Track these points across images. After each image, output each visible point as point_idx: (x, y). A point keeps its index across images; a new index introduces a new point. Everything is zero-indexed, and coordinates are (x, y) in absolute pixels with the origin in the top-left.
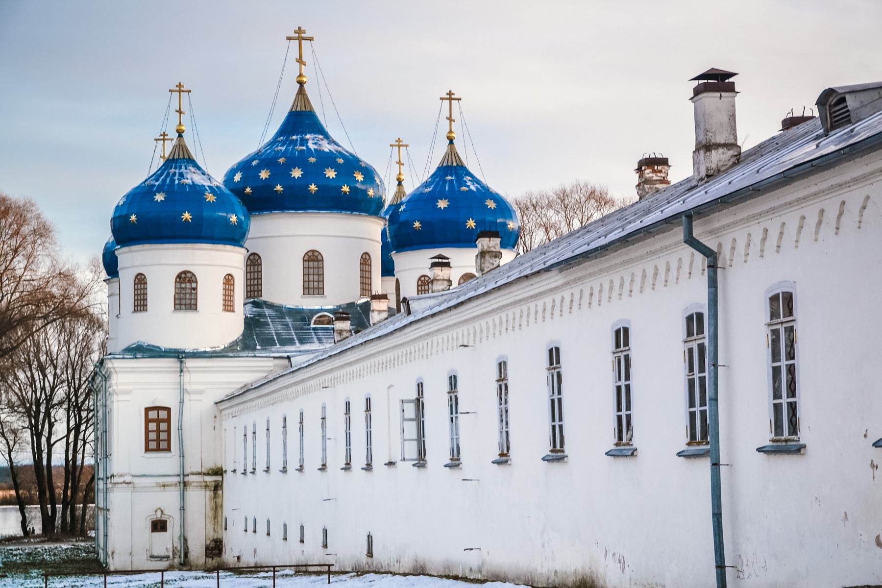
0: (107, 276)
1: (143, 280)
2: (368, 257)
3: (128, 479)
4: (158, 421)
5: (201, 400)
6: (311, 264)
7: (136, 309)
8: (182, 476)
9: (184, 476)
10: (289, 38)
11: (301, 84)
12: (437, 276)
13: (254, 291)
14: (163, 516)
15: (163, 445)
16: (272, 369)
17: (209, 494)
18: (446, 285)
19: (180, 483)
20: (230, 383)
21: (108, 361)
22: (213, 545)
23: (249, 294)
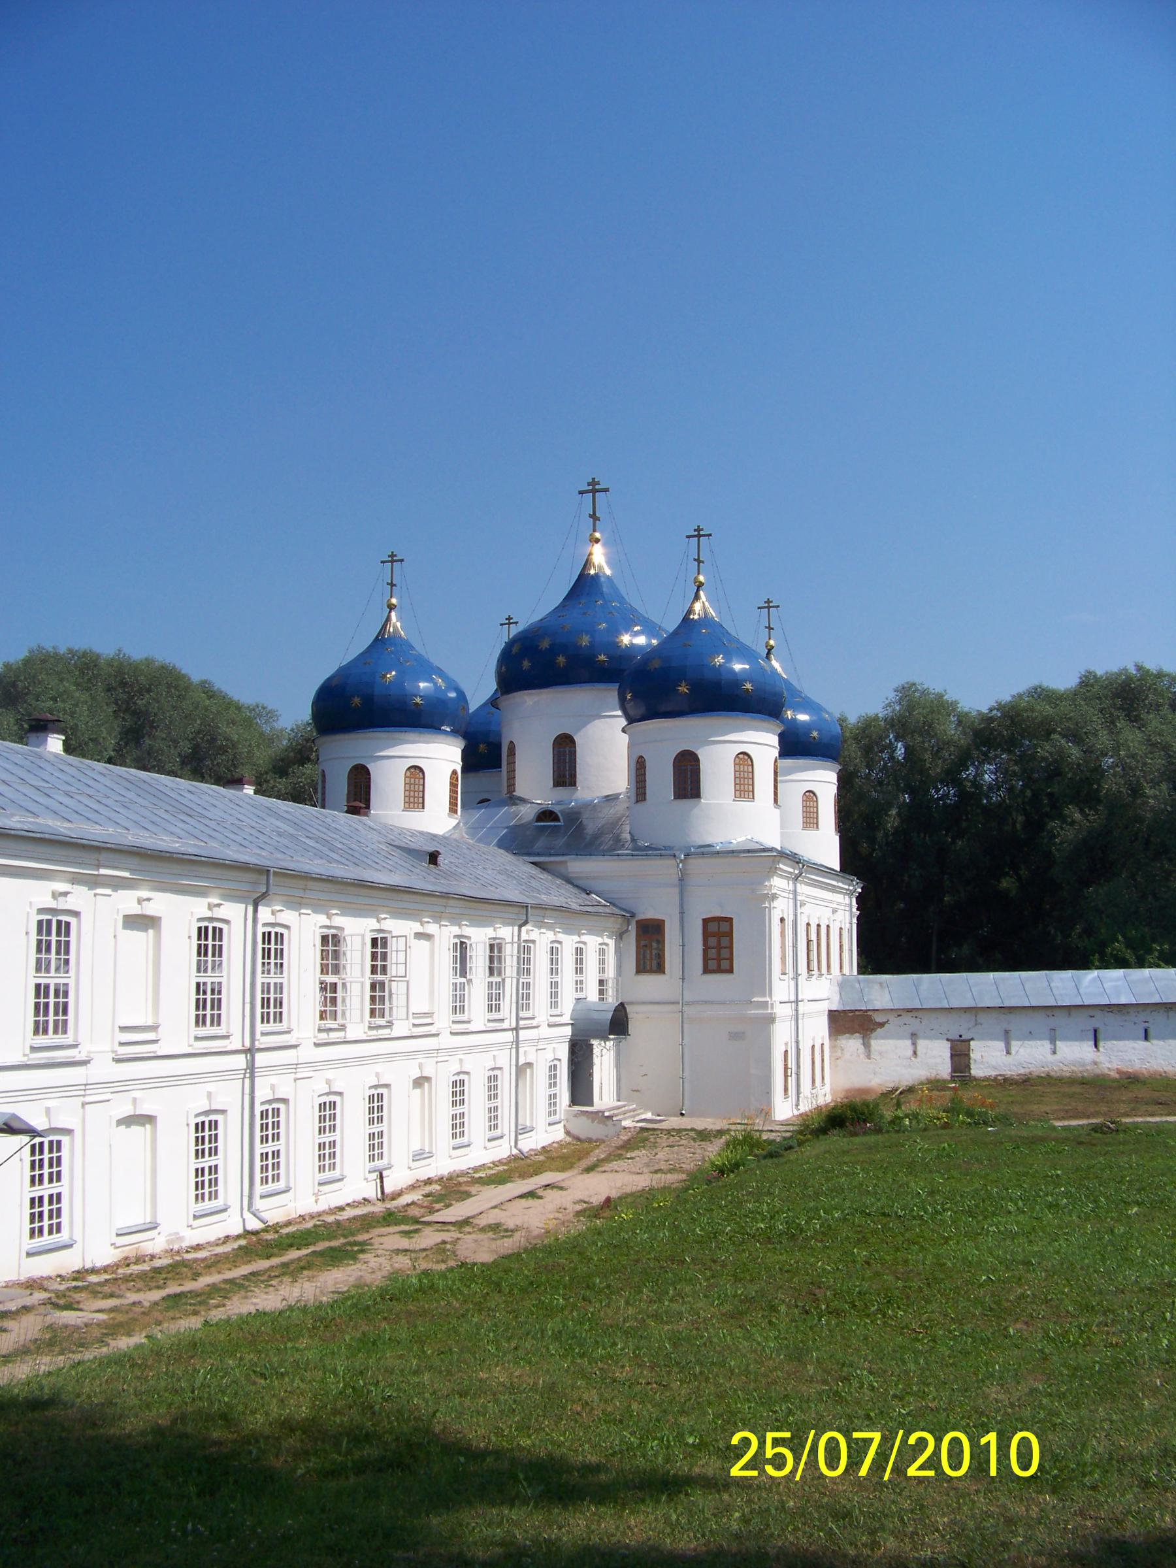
4: (719, 935)
15: (725, 964)
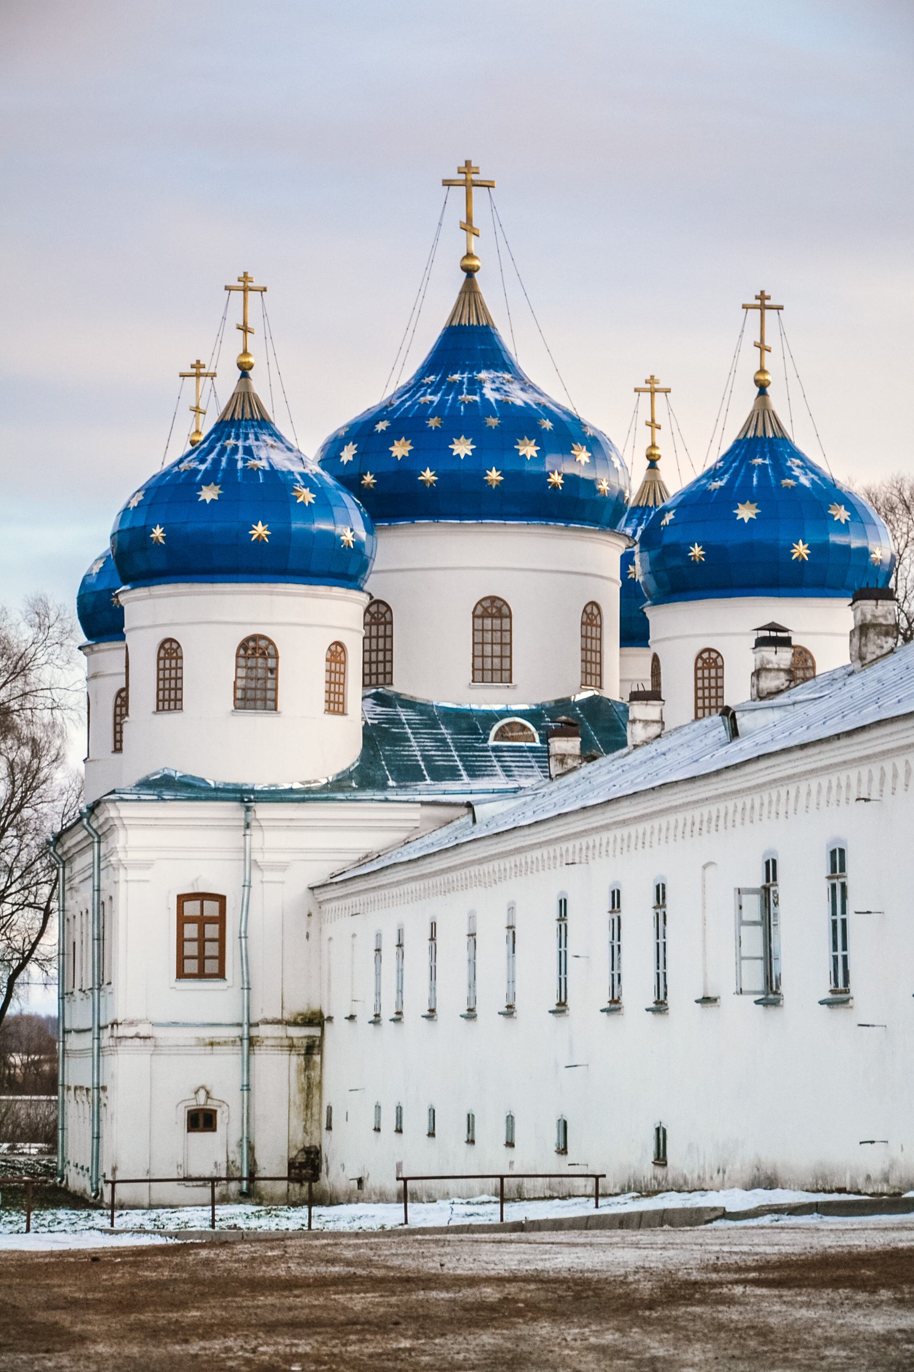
0: (86, 639)
1: (176, 651)
2: (595, 611)
3: (144, 1030)
4: (202, 921)
5: (283, 882)
6: (488, 622)
7: (161, 708)
8: (246, 1027)
9: (250, 1025)
10: (448, 183)
11: (470, 272)
12: (768, 663)
13: (377, 674)
14: (209, 1101)
15: (211, 966)
16: (417, 824)
17: (297, 1061)
18: (783, 680)
19: (241, 1039)
20: (339, 851)
21: (109, 805)
22: (301, 1158)
23: (367, 678)
